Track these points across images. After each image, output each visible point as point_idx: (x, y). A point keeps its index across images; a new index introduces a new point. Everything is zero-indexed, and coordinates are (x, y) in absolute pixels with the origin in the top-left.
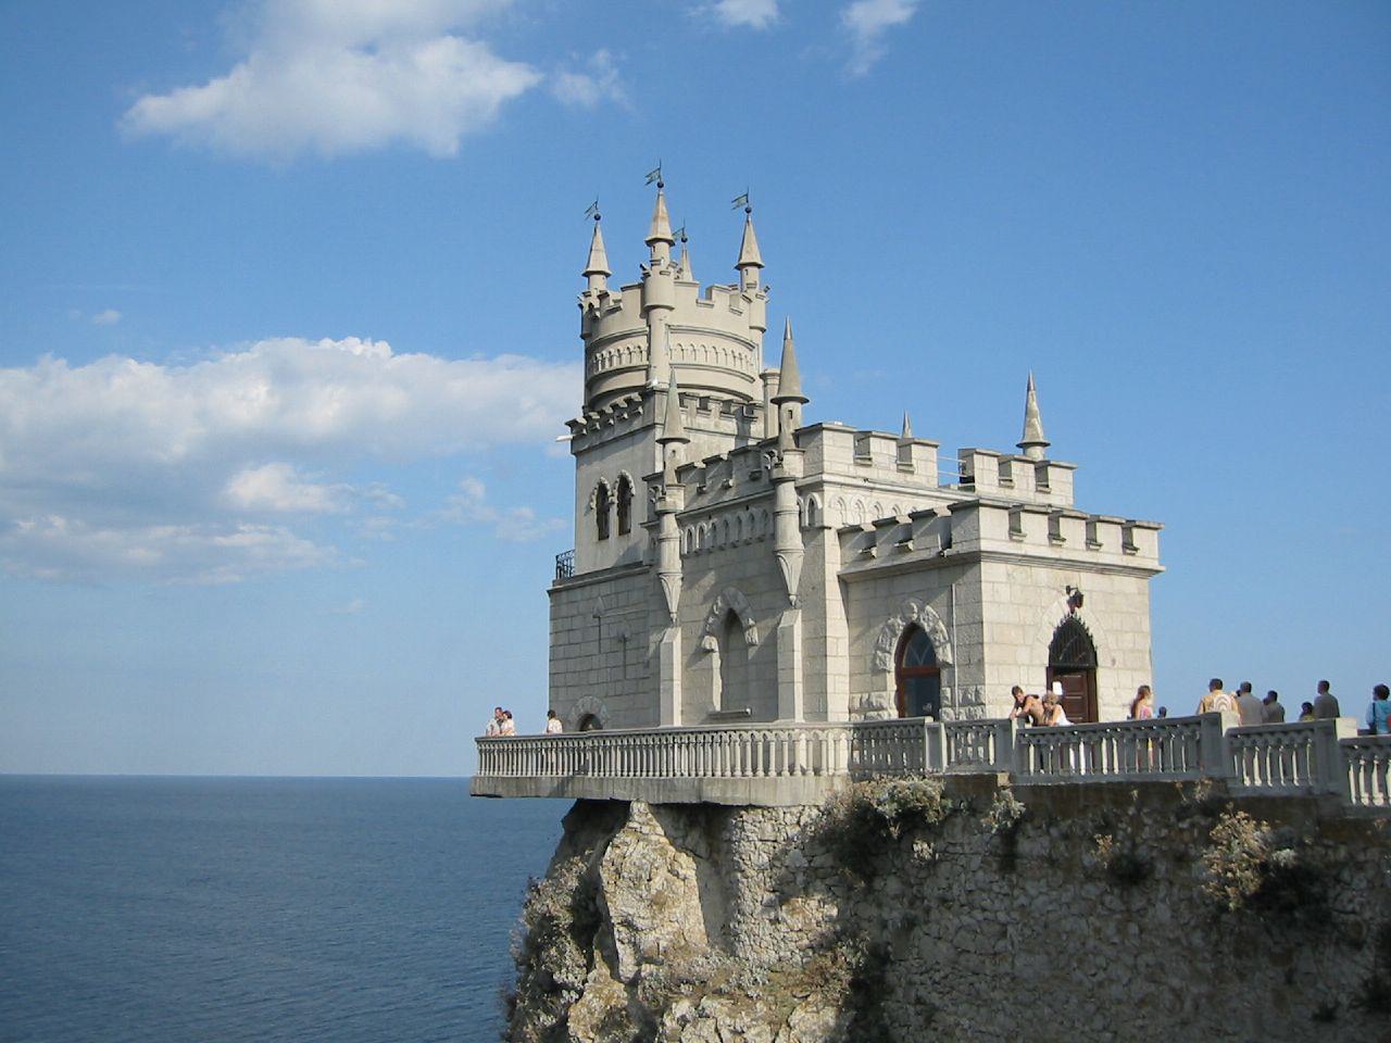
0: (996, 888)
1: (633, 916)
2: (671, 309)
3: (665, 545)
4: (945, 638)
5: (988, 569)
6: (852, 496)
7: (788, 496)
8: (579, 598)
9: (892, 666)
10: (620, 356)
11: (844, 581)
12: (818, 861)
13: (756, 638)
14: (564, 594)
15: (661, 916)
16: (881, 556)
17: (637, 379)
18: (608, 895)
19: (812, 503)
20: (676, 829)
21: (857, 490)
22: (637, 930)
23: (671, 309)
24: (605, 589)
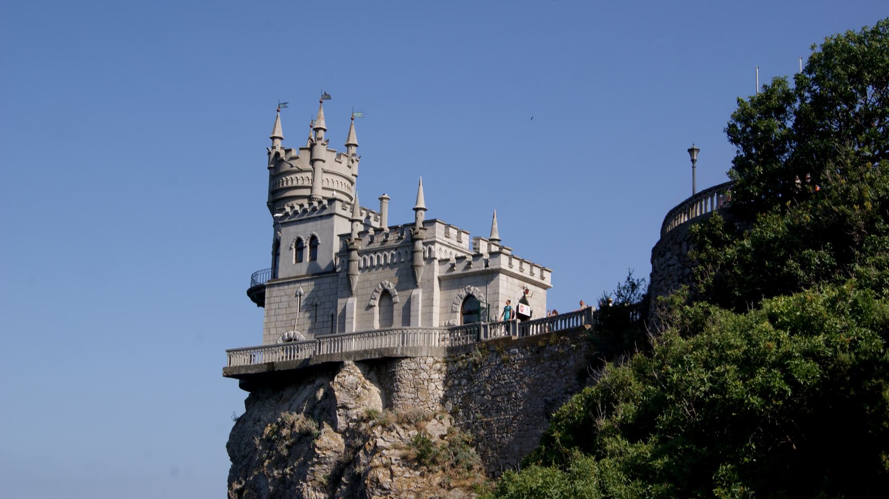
2: (324, 161)
3: (352, 263)
5: (502, 277)
6: (444, 248)
7: (419, 245)
9: (459, 309)
11: (440, 279)
12: (432, 377)
13: (398, 300)
16: (459, 269)
17: (307, 192)
19: (430, 249)
21: (446, 246)
22: (348, 409)
23: (324, 161)
24: (303, 284)
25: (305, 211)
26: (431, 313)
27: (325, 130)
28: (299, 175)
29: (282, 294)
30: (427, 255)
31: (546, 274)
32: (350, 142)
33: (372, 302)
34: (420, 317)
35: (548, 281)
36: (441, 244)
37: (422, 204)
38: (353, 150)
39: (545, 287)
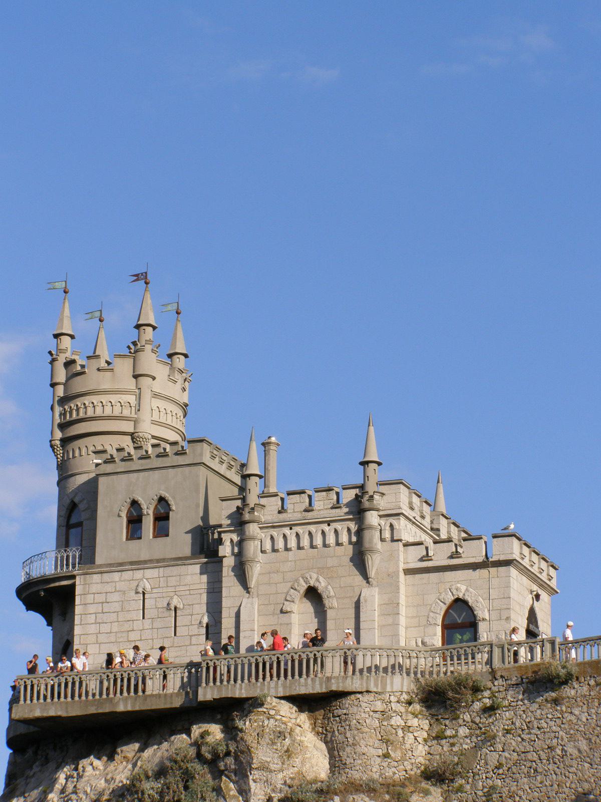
0: (550, 716)
1: (268, 763)
2: (154, 378)
4: (482, 605)
6: (409, 525)
7: (372, 518)
8: (117, 579)
9: (440, 621)
10: (86, 408)
13: (335, 604)
14: (95, 576)
15: (288, 762)
18: (252, 749)
20: (292, 713)
22: (271, 771)
23: (154, 378)
24: (149, 573)
25: (128, 459)
26: (396, 624)
27: (154, 328)
28: (114, 398)
29: (109, 588)
30: (387, 535)
31: (552, 572)
32: (178, 351)
33: (288, 607)
34: (376, 631)
35: (553, 584)
36: (407, 518)
37: (373, 456)
38: (180, 362)
39: (552, 592)
